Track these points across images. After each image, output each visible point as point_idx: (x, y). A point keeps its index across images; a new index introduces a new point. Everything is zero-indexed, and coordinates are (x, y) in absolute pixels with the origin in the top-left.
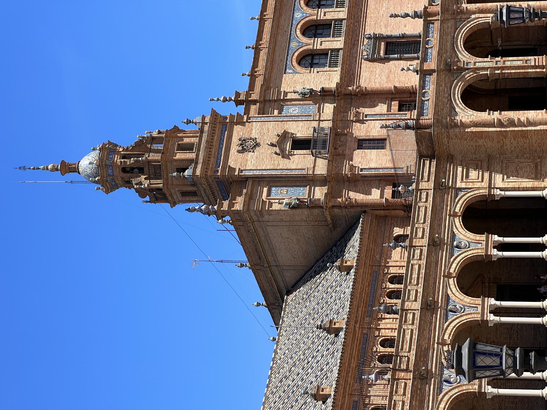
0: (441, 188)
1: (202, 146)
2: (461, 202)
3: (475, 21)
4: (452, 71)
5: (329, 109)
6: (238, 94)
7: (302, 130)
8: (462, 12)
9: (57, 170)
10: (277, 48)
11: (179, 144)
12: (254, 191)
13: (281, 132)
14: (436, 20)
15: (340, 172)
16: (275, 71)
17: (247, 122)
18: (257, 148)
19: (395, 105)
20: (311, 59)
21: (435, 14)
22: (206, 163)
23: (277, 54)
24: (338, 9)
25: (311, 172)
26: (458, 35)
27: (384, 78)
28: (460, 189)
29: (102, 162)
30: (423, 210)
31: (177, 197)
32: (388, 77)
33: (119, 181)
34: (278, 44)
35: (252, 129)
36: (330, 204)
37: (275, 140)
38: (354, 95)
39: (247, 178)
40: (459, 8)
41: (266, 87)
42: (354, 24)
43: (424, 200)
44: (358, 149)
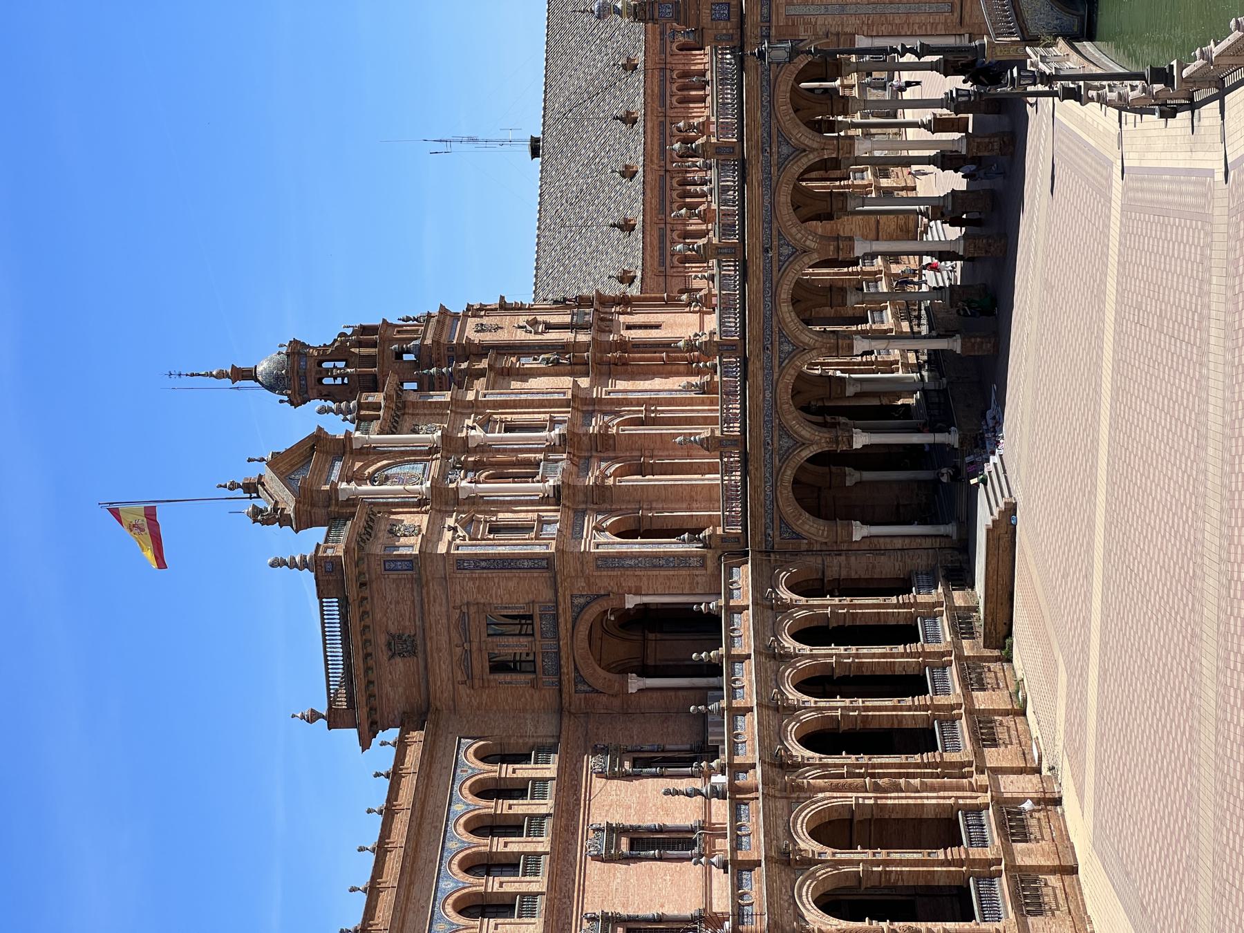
4: (792, 863)
8: (800, 788)
14: (752, 799)
21: (749, 790)
24: (528, 878)
26: (796, 818)
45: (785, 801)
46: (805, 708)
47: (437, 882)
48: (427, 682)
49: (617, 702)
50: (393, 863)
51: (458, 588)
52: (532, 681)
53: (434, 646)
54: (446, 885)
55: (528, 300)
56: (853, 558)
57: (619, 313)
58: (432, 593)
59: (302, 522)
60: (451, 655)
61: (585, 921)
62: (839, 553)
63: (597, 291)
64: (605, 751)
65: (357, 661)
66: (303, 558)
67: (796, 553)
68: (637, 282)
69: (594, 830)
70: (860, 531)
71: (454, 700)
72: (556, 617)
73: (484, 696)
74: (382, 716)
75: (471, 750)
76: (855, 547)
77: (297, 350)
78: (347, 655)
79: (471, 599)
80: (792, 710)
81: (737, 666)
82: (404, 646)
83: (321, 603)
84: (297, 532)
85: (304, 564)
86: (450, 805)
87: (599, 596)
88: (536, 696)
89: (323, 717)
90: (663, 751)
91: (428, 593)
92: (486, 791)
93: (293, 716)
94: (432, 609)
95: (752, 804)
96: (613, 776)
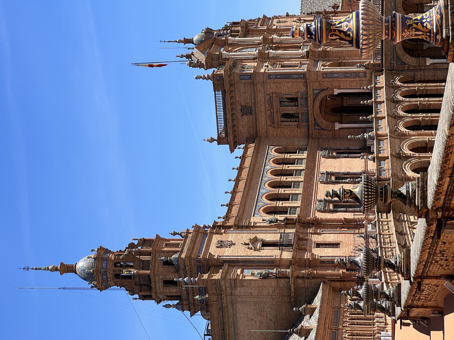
0: (398, 221)
1: (186, 244)
4: (402, 157)
6: (215, 222)
9: (56, 269)
10: (247, 204)
11: (166, 244)
12: (230, 271)
13: (252, 236)
14: (385, 139)
15: (303, 257)
17: (224, 233)
18: (233, 246)
21: (384, 136)
22: (191, 250)
25: (278, 257)
29: (99, 256)
31: (159, 288)
33: (110, 275)
36: (295, 274)
38: (312, 224)
39: (225, 261)
41: (239, 218)
45: (399, 140)
46: (407, 117)
47: (259, 190)
48: (256, 125)
49: (330, 133)
50: (242, 185)
51: (269, 87)
52: (297, 124)
53: (259, 111)
54: (262, 191)
55: (298, 13)
56: (426, 72)
57: (333, 16)
58: (258, 89)
59: (208, 66)
60: (266, 114)
61: (317, 202)
62: (421, 70)
63: (324, 9)
64: (326, 149)
65: (229, 117)
66: (208, 76)
67: (403, 71)
68: (340, 8)
69: (321, 174)
70: (429, 62)
71: (267, 133)
72: (307, 98)
73: (279, 131)
74: (239, 139)
75: (273, 150)
76: (428, 68)
77: (209, 32)
78: (225, 114)
79: (274, 91)
80: (401, 118)
81: (379, 105)
82: (247, 110)
83: (215, 93)
84: (206, 70)
85: (208, 78)
86: (265, 166)
87: (324, 90)
88: (299, 131)
89: (216, 140)
90: (349, 149)
91: (257, 89)
92: (278, 162)
93: (204, 140)
94: (258, 95)
95: (385, 141)
96: (329, 157)
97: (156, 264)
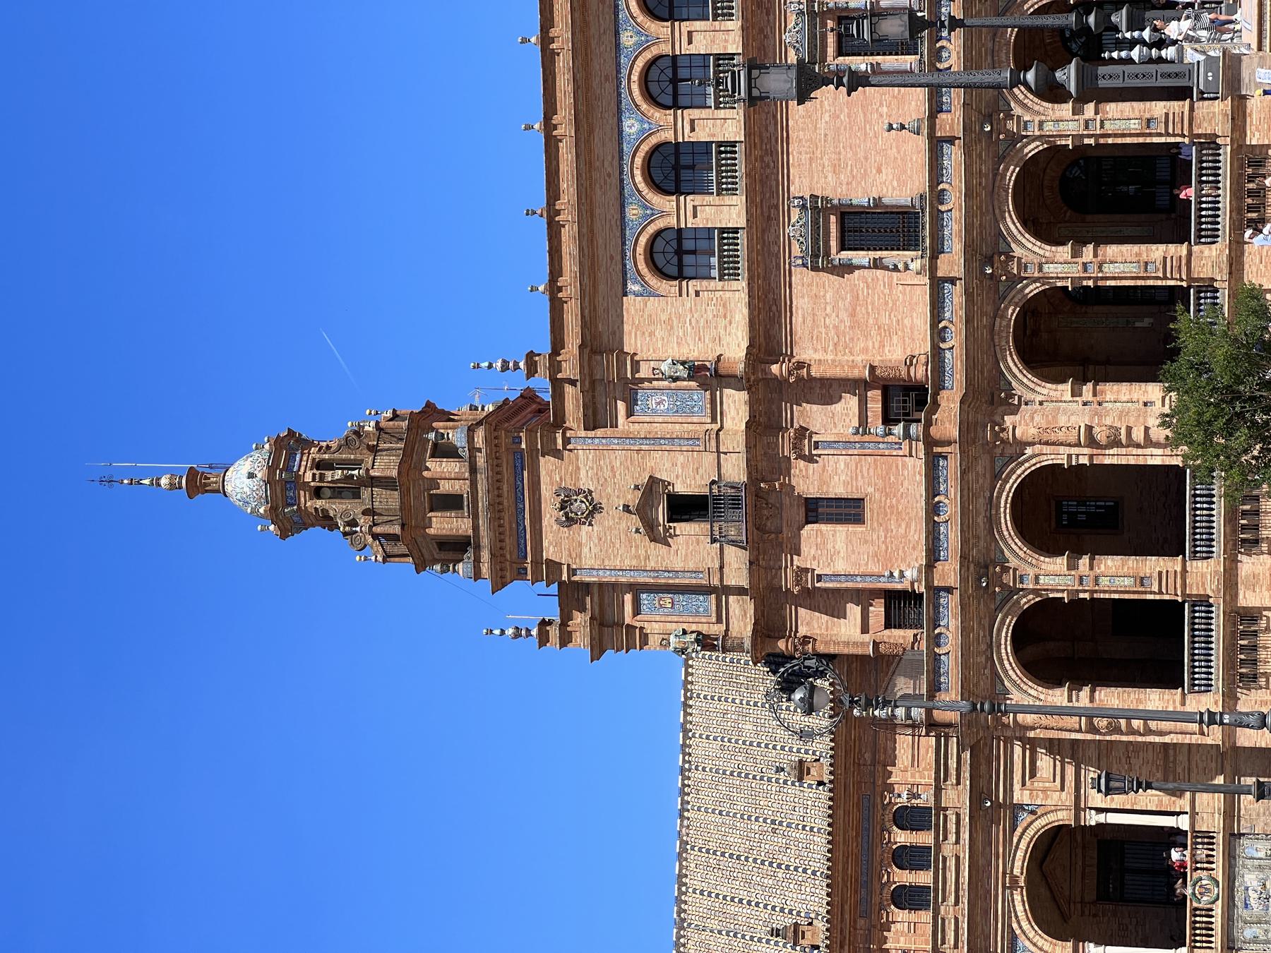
2: (1023, 845)
3: (1034, 461)
5: (736, 406)
7: (688, 478)
10: (598, 225)
15: (775, 581)
16: (602, 287)
18: (597, 516)
19: (877, 610)
20: (678, 257)
23: (600, 241)
27: (844, 315)
28: (1021, 807)
30: (951, 863)
32: (853, 315)
34: (597, 211)
35: (578, 468)
37: (634, 499)
40: (996, 435)
42: (762, 161)
43: (952, 838)
44: (808, 522)
97: (424, 551)
